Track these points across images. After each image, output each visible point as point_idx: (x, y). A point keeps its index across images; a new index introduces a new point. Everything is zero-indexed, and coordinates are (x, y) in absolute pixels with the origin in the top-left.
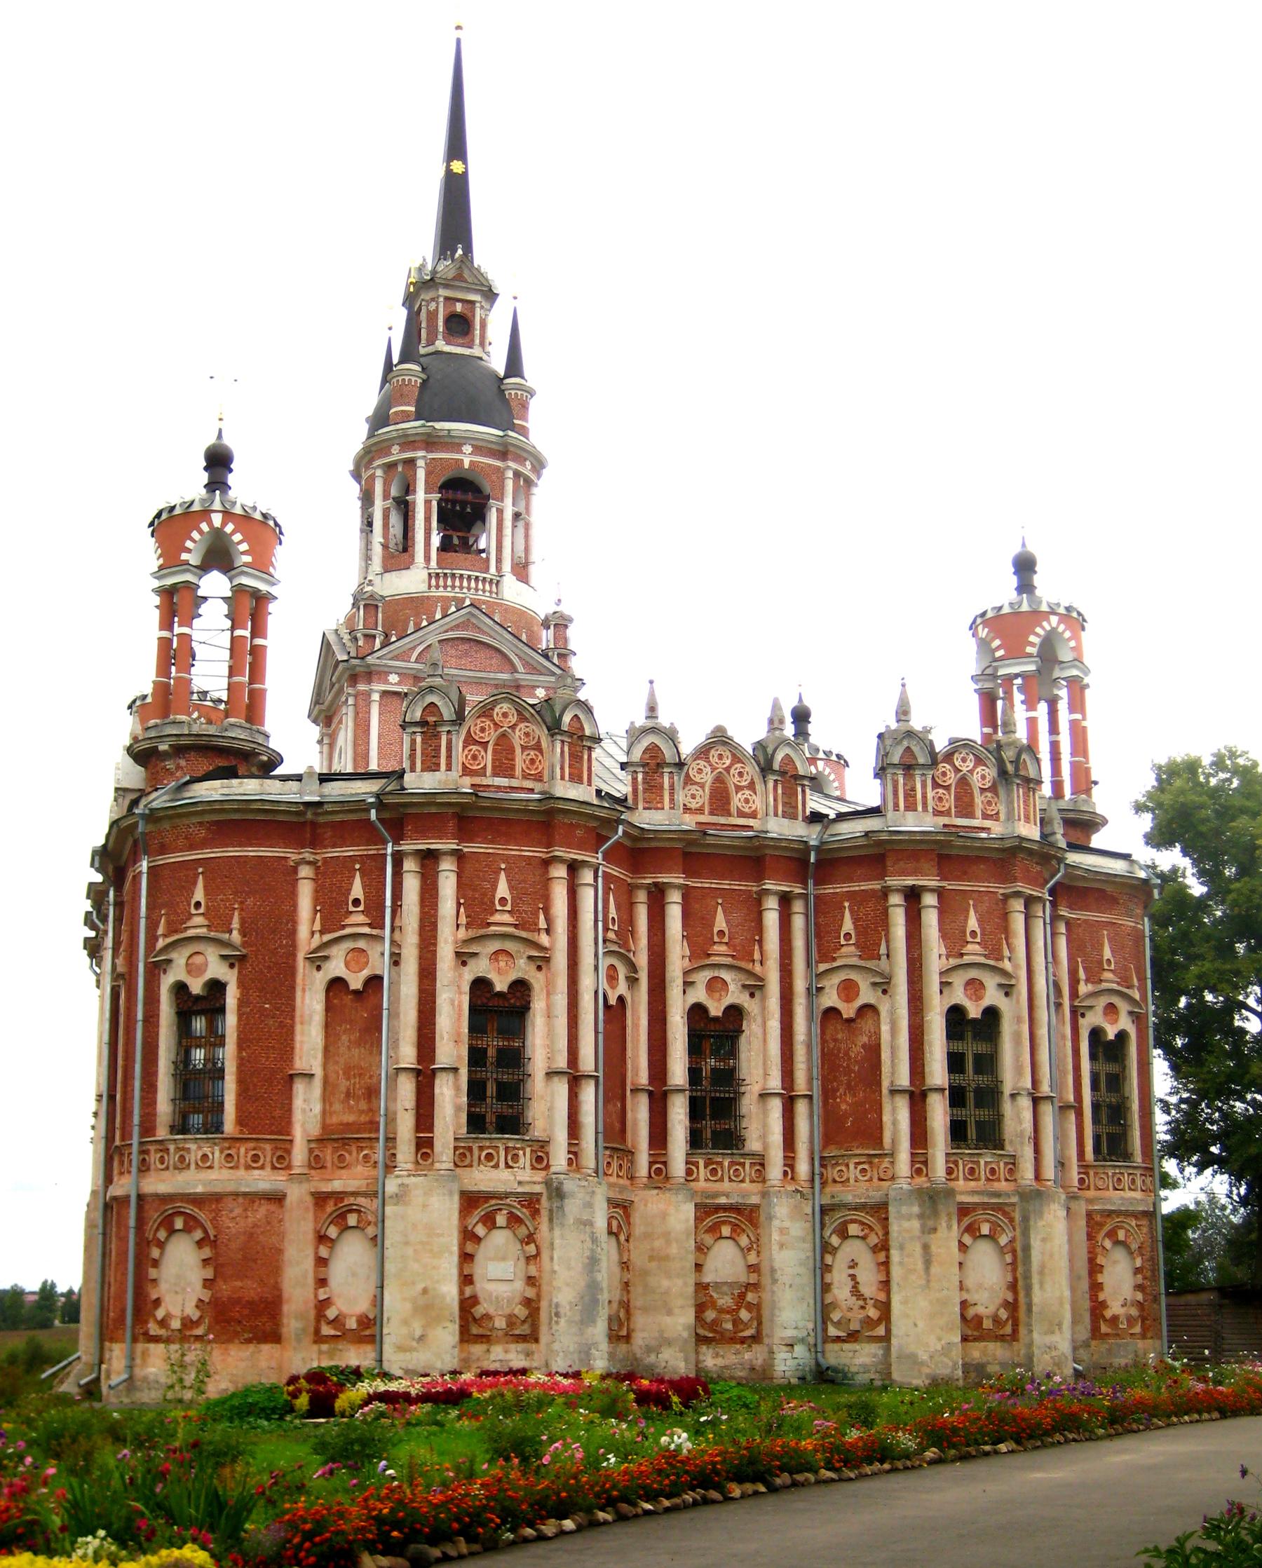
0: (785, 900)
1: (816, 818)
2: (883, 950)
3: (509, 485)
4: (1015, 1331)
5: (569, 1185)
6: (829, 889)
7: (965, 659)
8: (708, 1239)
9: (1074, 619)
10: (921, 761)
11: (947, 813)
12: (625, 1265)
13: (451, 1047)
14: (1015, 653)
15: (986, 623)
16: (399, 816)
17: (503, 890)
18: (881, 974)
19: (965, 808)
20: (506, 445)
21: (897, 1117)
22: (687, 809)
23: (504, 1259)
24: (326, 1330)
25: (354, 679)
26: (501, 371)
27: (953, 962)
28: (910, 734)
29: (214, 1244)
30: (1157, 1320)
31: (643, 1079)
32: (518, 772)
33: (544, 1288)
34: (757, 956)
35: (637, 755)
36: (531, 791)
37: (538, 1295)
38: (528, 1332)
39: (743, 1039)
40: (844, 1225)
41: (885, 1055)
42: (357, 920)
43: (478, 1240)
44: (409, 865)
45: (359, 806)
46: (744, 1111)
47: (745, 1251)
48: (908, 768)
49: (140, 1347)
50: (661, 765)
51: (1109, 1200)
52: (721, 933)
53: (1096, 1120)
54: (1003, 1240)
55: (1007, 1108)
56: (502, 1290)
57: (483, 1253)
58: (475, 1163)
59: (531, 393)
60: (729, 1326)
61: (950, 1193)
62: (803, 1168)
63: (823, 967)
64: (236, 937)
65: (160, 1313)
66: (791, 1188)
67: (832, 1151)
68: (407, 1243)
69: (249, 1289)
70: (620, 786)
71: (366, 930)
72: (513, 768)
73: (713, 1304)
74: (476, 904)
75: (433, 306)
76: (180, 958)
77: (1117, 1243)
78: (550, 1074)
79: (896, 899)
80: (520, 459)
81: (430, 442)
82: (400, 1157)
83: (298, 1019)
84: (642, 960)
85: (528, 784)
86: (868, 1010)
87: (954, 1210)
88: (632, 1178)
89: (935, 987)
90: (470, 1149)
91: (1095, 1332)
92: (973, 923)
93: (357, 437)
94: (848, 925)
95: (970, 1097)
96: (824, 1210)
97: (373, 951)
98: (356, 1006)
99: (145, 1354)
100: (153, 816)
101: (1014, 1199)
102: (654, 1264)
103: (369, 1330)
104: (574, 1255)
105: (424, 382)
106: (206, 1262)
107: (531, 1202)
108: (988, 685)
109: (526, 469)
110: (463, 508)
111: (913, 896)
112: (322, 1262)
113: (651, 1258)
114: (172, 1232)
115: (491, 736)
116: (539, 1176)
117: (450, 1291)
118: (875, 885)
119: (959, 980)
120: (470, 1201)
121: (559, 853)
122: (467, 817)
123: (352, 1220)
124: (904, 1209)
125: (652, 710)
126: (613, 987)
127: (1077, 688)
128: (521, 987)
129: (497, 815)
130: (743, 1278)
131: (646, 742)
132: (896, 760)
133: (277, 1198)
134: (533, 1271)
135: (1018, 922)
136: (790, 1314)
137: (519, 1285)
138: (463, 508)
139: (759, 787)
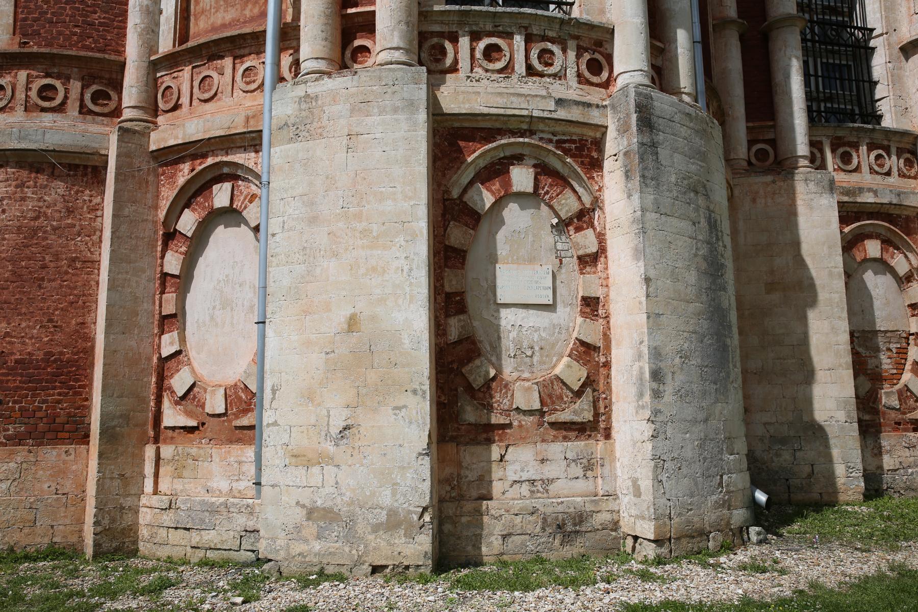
37: (606, 337)
38: (588, 416)
43: (473, 218)
58: (464, 63)
68: (313, 220)
102: (776, 297)
113: (771, 287)
116: (595, 95)
117: (409, 320)
123: (221, 196)
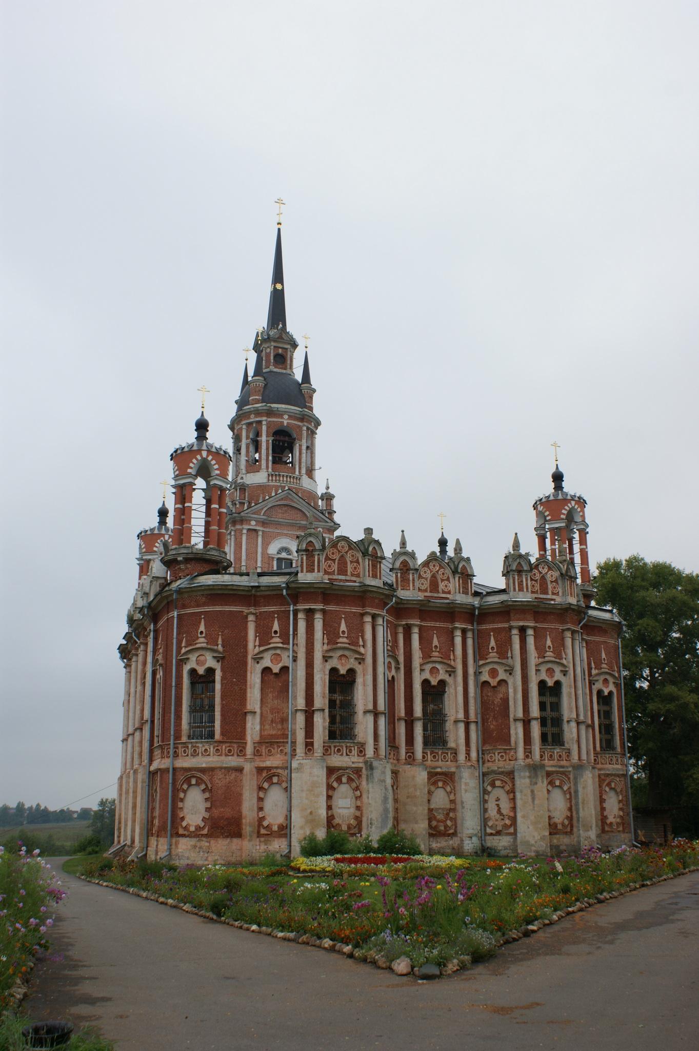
0: (464, 631)
1: (476, 594)
2: (509, 655)
3: (305, 433)
4: (572, 830)
5: (375, 764)
6: (484, 627)
7: (531, 519)
8: (433, 788)
9: (582, 502)
10: (525, 568)
11: (536, 592)
12: (396, 801)
13: (321, 700)
14: (556, 518)
15: (541, 504)
16: (297, 593)
17: (343, 627)
18: (509, 666)
19: (544, 590)
20: (304, 415)
21: (517, 731)
22: (419, 590)
23: (346, 798)
24: (263, 831)
25: (234, 523)
26: (300, 381)
27: (541, 660)
28: (520, 556)
29: (211, 791)
30: (629, 824)
31: (403, 714)
32: (349, 573)
33: (364, 811)
34: (452, 657)
35: (397, 565)
36: (355, 582)
39: (446, 695)
40: (494, 781)
41: (511, 703)
42: (276, 641)
43: (334, 789)
44: (301, 615)
45: (278, 588)
46: (447, 728)
47: (449, 794)
48: (520, 572)
49: (174, 840)
50: (409, 569)
51: (608, 770)
52: (436, 646)
53: (600, 732)
54: (565, 788)
55: (565, 727)
56: (345, 812)
57: (336, 795)
59: (314, 391)
60: (442, 828)
61: (543, 766)
62: (474, 755)
63: (481, 662)
64: (220, 648)
65: (184, 824)
66: (469, 764)
67: (487, 747)
69: (228, 812)
70: (391, 578)
71: (281, 645)
72: (346, 571)
73: (435, 818)
74: (331, 634)
75: (268, 350)
76: (193, 657)
77: (611, 789)
78: (365, 712)
79: (515, 632)
80: (310, 422)
81: (270, 413)
82: (298, 751)
83: (248, 686)
84: (401, 659)
85: (354, 579)
86: (503, 682)
87: (544, 774)
88: (398, 760)
89: (534, 672)
90: (330, 747)
91: (603, 831)
92: (549, 643)
93: (232, 411)
94: (493, 643)
95: (549, 722)
96: (484, 775)
97: (284, 655)
98: (277, 680)
99: (177, 844)
100: (179, 591)
101: (570, 769)
102: (409, 800)
103: (284, 831)
104: (376, 797)
105: (266, 385)
106: (207, 799)
107: (358, 771)
108: (542, 532)
109: (312, 426)
110: (284, 444)
111: (523, 630)
112: (260, 799)
113: (408, 797)
114: (190, 785)
115: (337, 557)
116: (361, 759)
117: (323, 812)
118: (506, 625)
119: (543, 669)
120: (331, 771)
121: (368, 610)
122: (327, 593)
123: (275, 780)
124: (522, 774)
125: (403, 544)
126: (390, 671)
127: (583, 534)
128: (352, 672)
129: (339, 593)
130: (448, 806)
131: (401, 559)
132: (514, 568)
133: (240, 770)
134: (359, 803)
135: (568, 642)
136: (470, 823)
137: (353, 810)
138: (283, 444)
139: (451, 579)
